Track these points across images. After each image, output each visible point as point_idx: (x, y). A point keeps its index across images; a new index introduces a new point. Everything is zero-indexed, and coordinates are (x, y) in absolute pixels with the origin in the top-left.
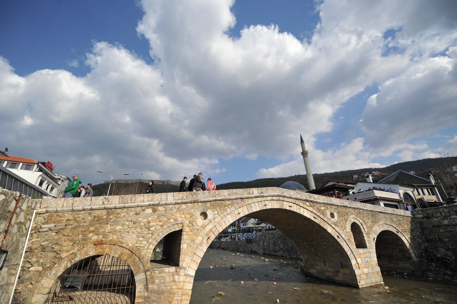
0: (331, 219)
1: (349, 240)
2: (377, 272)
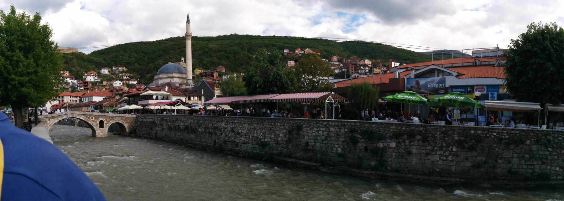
0: (91, 120)
1: (97, 125)
2: (106, 135)
